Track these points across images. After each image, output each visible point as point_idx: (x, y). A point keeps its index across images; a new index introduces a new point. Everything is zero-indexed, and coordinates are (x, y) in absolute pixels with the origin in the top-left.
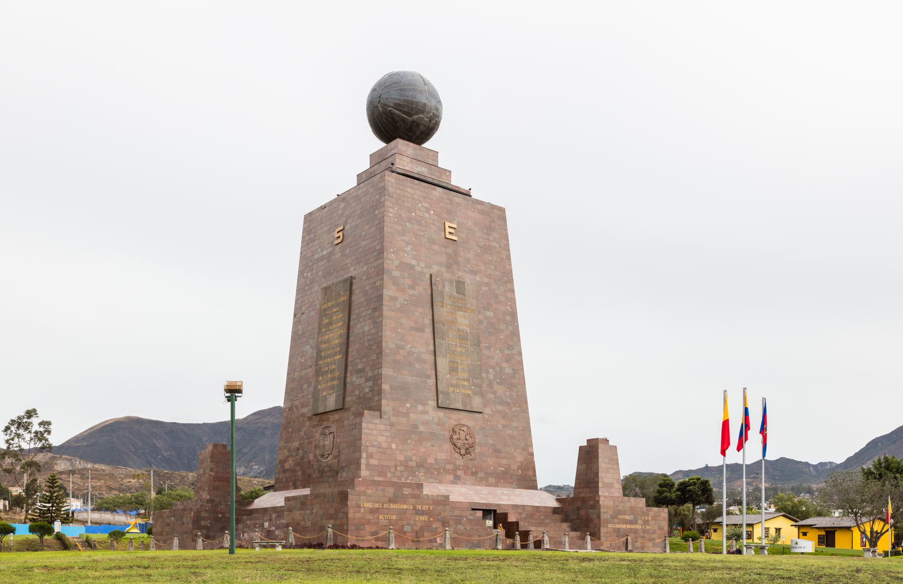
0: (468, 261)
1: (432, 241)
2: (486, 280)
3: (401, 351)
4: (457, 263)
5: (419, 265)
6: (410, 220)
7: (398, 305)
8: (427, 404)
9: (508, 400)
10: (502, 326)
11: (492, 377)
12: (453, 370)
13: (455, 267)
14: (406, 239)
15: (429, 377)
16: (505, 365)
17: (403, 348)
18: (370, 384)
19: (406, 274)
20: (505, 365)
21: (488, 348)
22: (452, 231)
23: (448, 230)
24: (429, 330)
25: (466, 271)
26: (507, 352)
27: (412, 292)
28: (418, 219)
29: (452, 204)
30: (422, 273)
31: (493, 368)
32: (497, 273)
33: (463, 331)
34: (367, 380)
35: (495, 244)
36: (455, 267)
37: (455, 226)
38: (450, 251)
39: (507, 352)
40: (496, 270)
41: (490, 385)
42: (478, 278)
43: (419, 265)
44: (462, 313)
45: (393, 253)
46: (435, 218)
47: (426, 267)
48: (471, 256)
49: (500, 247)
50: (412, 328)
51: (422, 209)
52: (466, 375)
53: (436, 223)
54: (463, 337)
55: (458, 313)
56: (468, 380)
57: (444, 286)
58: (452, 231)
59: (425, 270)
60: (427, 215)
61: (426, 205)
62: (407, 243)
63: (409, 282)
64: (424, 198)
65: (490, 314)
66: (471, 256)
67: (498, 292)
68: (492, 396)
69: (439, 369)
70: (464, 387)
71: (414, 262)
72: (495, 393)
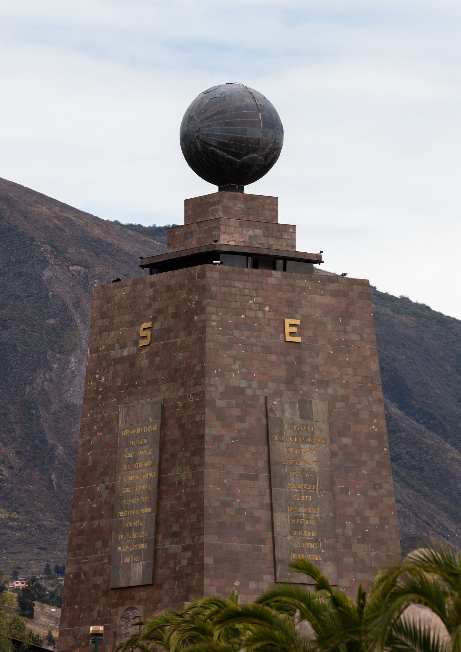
0: (315, 368)
1: (267, 350)
2: (341, 392)
3: (228, 510)
4: (301, 374)
5: (250, 387)
6: (237, 325)
7: (223, 447)
8: (262, 580)
9: (374, 564)
10: (364, 457)
11: (350, 533)
12: (296, 527)
13: (298, 381)
14: (233, 353)
15: (263, 541)
16: (368, 513)
17: (229, 505)
18: (188, 554)
19: (234, 402)
20: (368, 513)
21: (345, 491)
22: (294, 330)
23: (288, 329)
24: (263, 476)
25: (313, 384)
26: (371, 493)
27: (240, 426)
28: (249, 321)
29: (293, 291)
30: (255, 397)
31: (352, 518)
32: (357, 379)
33: (309, 471)
34: (185, 549)
35: (354, 337)
36: (298, 381)
37: (298, 322)
38: (291, 358)
39: (371, 493)
40: (355, 374)
41: (348, 545)
42: (330, 391)
43: (250, 387)
44: (307, 446)
45: (216, 375)
46: (271, 315)
47: (260, 387)
48: (320, 360)
49: (362, 339)
50: (242, 476)
51: (253, 306)
52: (314, 534)
53: (273, 323)
54: (308, 479)
55: (302, 446)
56: (315, 541)
57: (283, 412)
58: (294, 330)
59: (258, 392)
60: (260, 314)
61: (259, 300)
62: (235, 359)
63: (237, 412)
64: (256, 290)
65: (347, 441)
66: (320, 360)
67: (358, 406)
68: (351, 560)
69: (277, 529)
70: (310, 551)
71: (243, 384)
72: (354, 555)
